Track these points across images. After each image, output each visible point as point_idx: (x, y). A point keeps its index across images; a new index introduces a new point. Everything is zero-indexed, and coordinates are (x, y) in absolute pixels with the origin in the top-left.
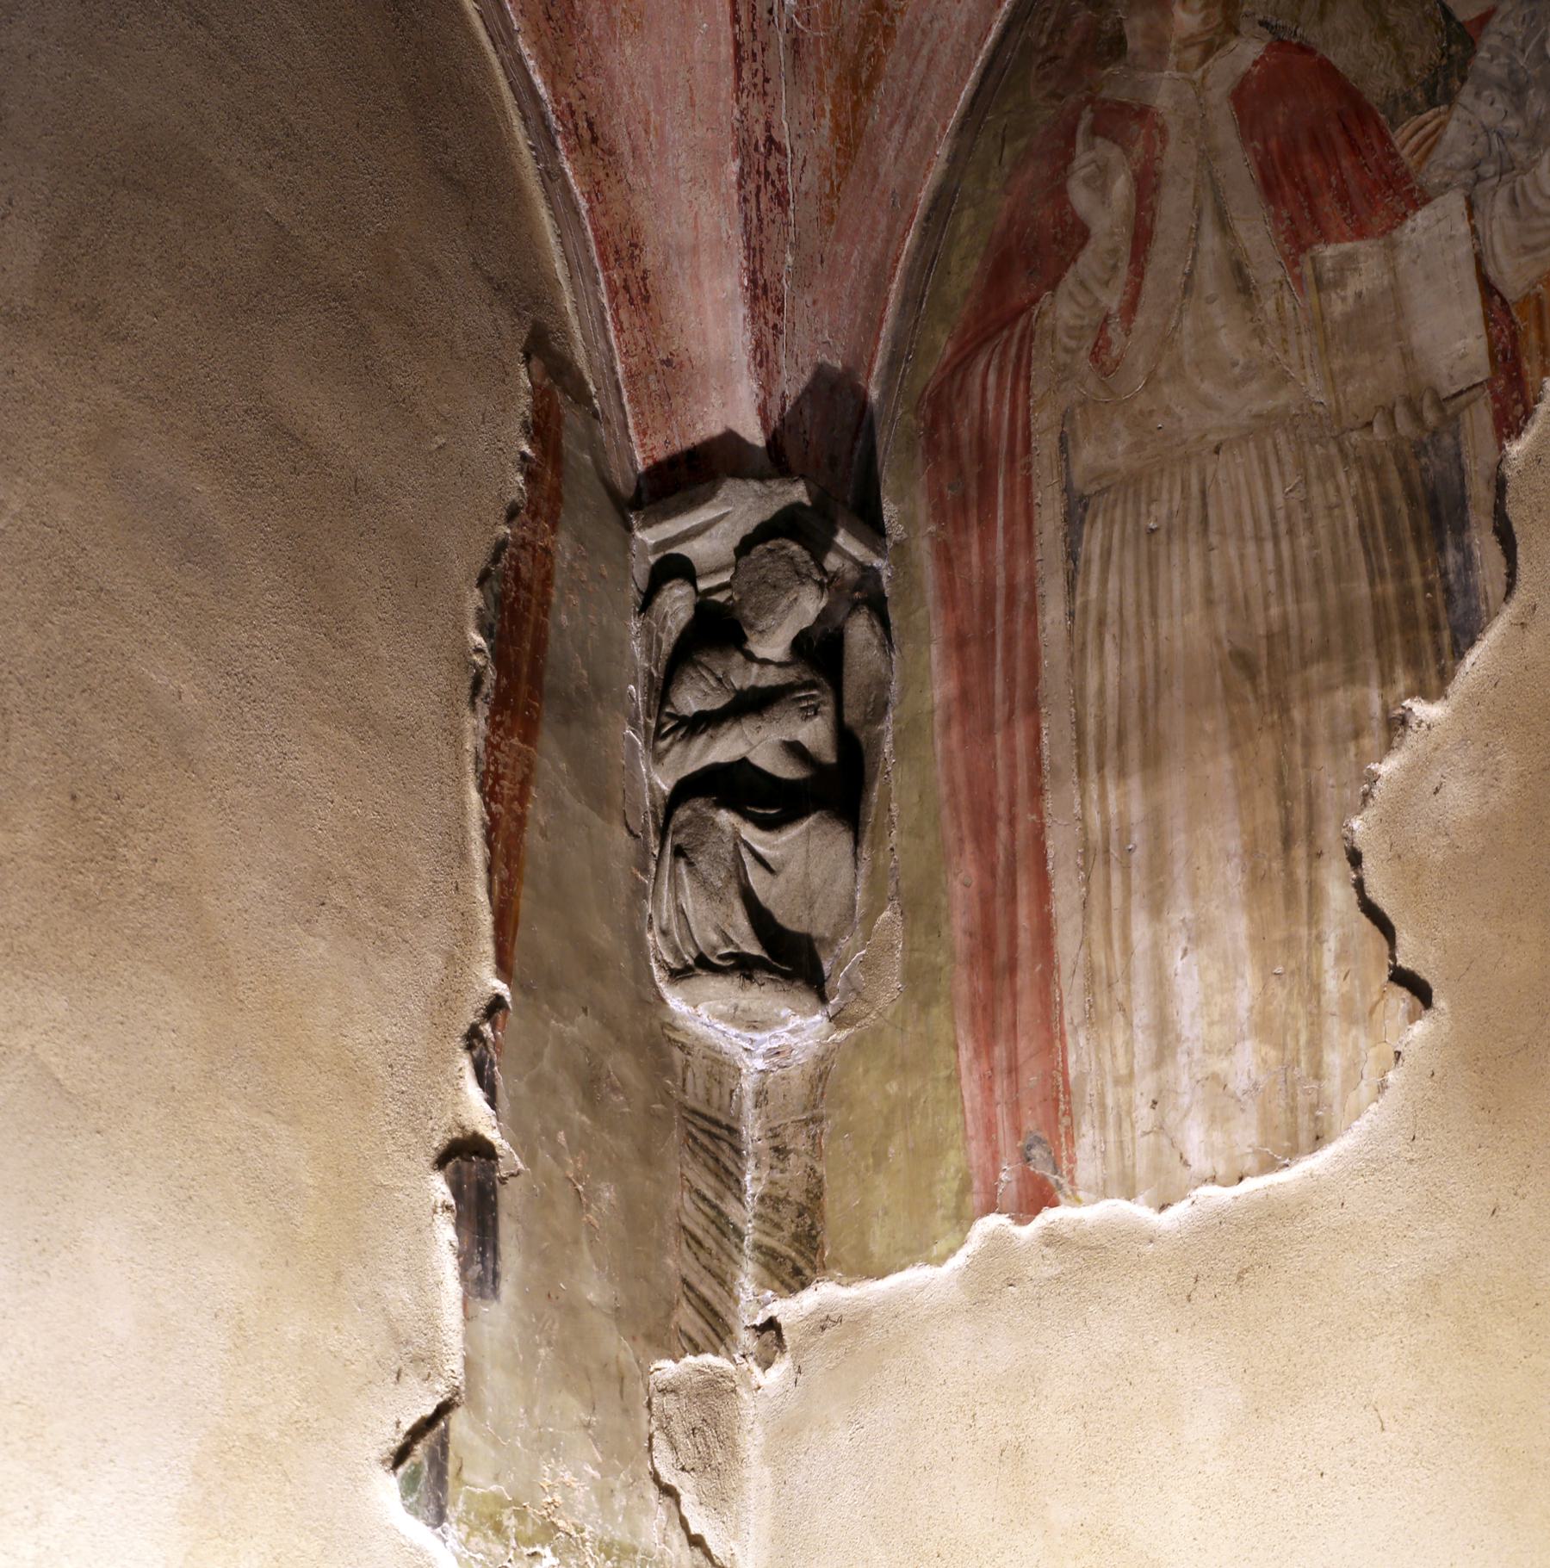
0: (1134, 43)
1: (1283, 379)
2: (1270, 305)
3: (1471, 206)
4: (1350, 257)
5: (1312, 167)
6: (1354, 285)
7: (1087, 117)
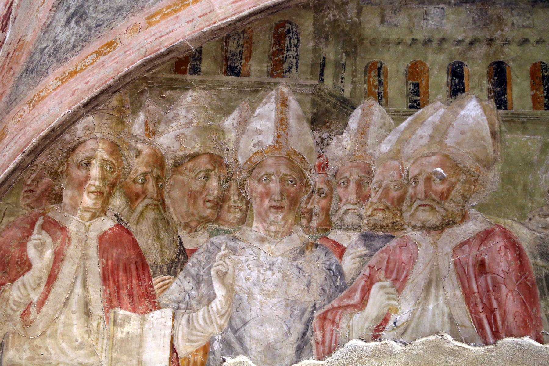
0: (65, 200)
1: (94, 353)
2: (95, 324)
3: (174, 317)
4: (128, 317)
5: (122, 278)
6: (127, 328)
7: (40, 221)
